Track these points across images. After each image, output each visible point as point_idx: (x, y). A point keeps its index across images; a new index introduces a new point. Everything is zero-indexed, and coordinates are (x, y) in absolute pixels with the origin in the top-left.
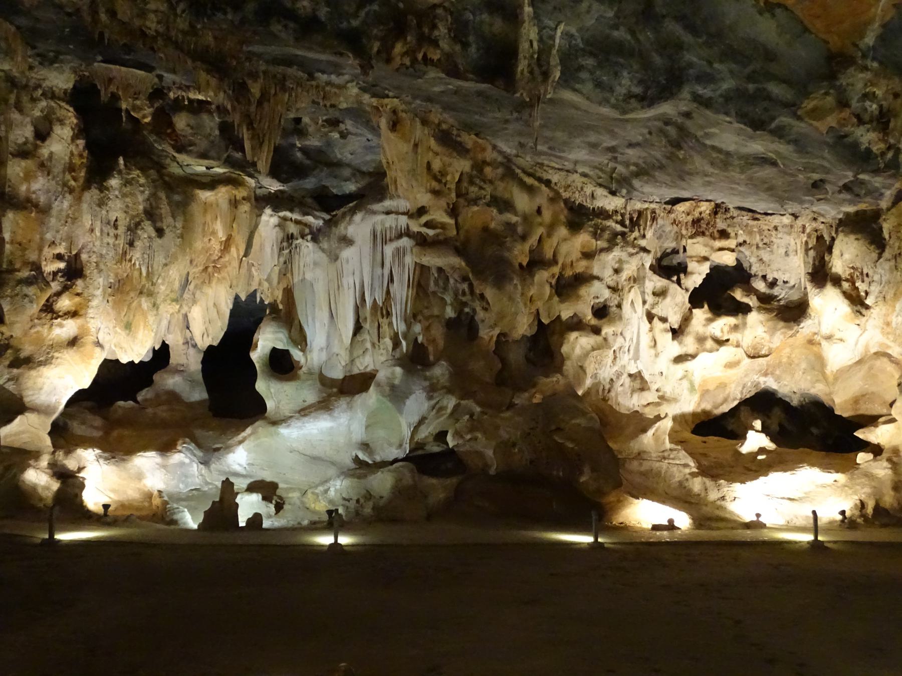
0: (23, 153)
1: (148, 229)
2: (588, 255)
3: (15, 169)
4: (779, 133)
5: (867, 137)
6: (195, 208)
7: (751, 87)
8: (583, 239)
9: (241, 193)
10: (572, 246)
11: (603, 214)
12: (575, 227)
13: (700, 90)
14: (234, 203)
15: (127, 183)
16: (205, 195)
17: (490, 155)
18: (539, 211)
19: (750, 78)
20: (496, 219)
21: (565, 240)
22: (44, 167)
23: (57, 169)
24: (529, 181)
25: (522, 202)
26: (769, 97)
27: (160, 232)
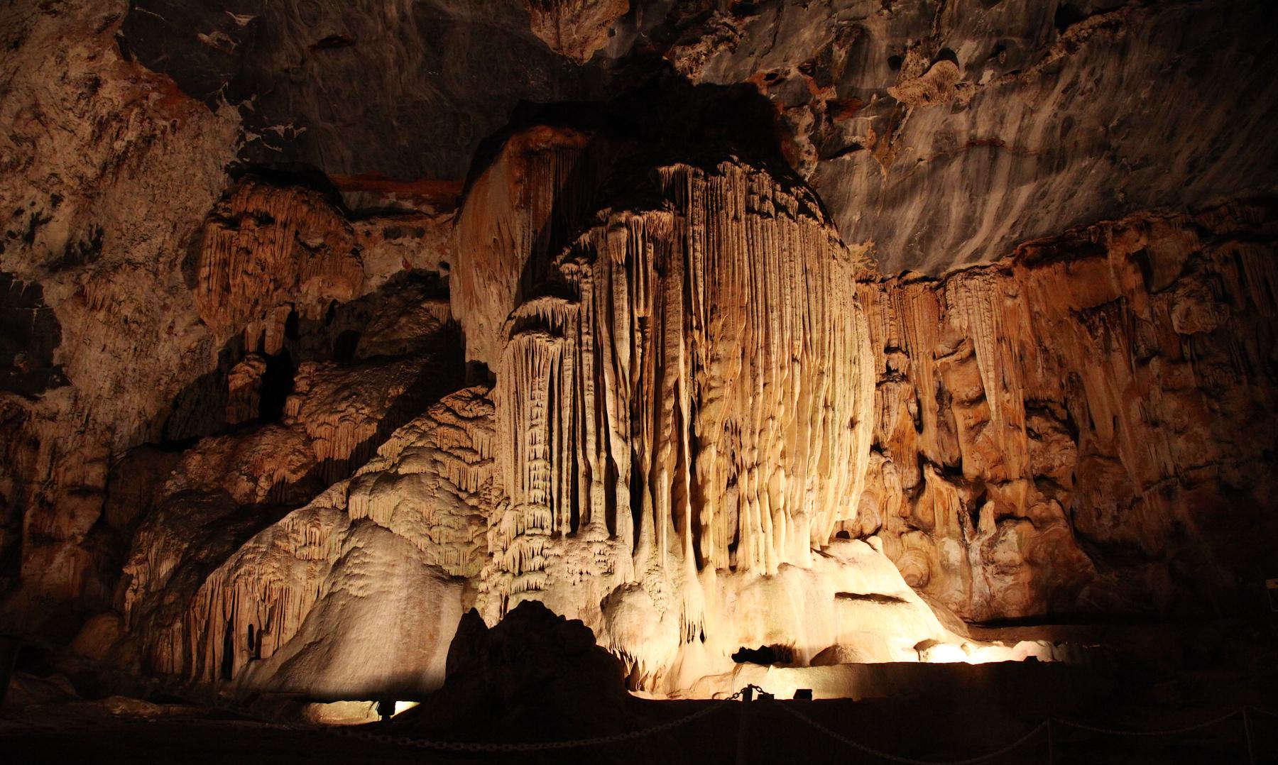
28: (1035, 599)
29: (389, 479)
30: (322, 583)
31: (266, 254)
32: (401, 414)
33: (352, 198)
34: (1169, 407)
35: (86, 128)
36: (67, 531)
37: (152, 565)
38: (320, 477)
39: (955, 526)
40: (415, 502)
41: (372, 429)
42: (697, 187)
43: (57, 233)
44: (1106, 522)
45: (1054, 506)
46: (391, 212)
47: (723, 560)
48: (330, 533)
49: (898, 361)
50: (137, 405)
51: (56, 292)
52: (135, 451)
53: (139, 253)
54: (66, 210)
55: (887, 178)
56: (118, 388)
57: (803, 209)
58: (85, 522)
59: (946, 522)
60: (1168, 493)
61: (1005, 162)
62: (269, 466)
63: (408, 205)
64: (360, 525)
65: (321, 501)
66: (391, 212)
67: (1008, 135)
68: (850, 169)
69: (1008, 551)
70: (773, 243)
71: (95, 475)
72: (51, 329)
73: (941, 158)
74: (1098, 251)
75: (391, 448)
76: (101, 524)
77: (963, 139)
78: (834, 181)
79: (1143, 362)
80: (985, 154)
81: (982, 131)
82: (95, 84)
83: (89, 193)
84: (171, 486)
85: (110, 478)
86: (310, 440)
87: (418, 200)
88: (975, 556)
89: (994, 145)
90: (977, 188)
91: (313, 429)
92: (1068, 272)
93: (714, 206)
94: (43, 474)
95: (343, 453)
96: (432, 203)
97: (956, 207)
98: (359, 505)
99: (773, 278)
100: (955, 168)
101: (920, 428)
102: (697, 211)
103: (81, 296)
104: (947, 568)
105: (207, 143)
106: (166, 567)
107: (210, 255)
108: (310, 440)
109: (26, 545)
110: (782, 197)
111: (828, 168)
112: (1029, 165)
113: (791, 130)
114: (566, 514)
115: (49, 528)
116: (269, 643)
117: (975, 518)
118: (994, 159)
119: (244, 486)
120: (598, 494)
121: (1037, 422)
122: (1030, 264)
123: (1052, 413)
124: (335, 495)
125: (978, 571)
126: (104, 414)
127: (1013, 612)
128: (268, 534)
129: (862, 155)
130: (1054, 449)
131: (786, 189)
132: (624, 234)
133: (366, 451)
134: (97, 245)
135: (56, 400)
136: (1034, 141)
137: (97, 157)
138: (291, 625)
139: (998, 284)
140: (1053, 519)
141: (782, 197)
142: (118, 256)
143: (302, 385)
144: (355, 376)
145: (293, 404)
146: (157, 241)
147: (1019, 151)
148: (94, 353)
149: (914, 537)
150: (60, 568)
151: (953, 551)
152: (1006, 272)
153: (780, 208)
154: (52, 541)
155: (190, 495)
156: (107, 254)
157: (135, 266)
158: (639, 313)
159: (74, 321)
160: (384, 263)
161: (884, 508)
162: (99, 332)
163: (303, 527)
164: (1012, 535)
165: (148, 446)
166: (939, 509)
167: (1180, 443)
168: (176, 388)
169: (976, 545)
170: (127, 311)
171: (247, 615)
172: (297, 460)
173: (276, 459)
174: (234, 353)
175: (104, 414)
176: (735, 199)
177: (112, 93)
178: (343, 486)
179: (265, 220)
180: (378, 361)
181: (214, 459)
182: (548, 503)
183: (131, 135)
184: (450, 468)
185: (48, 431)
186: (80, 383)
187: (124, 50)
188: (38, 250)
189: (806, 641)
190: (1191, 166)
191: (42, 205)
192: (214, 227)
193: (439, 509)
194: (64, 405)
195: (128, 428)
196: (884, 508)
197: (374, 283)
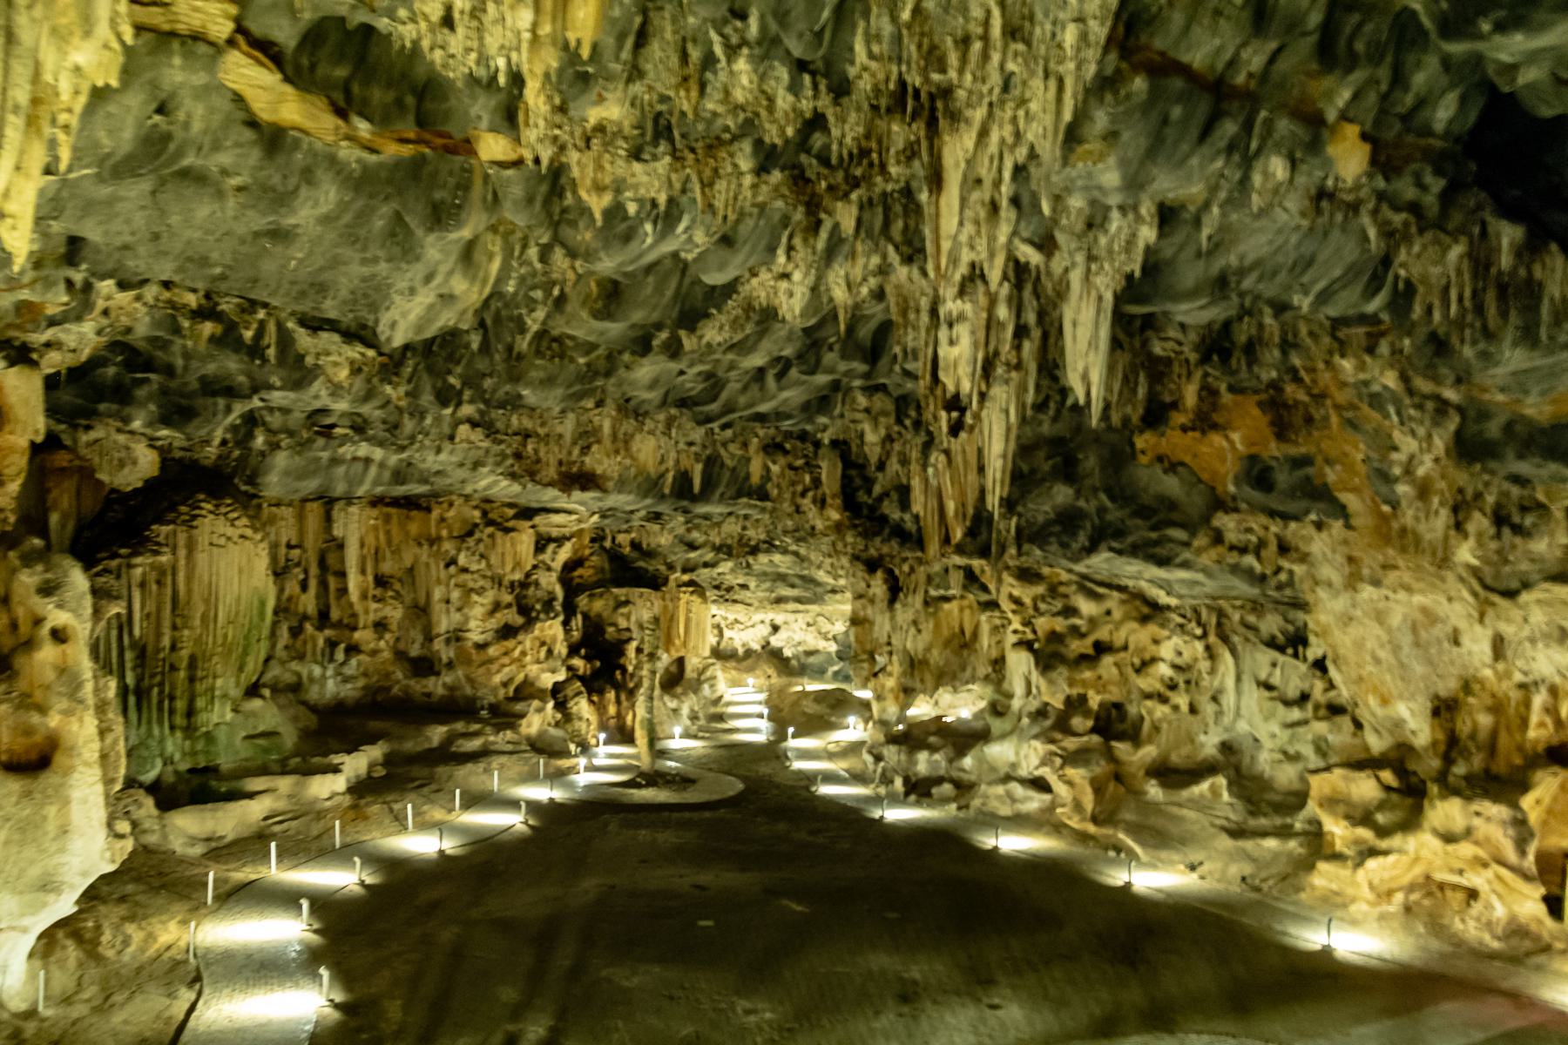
1: (913, 630)
2: (1156, 642)
4: (1185, 565)
5: (1249, 560)
6: (941, 614)
7: (1154, 535)
8: (1153, 629)
9: (966, 603)
10: (1138, 636)
11: (1168, 608)
12: (1144, 620)
13: (1115, 545)
14: (961, 610)
15: (904, 605)
16: (946, 606)
17: (1065, 576)
18: (1108, 613)
19: (1154, 528)
20: (1060, 624)
21: (1134, 631)
22: (872, 601)
23: (877, 600)
24: (1101, 590)
25: (1087, 607)
26: (1171, 540)
27: (919, 631)
39: (319, 658)
42: (182, 538)
59: (314, 653)
88: (329, 673)
93: (191, 547)
102: (182, 553)
104: (311, 680)
112: (387, 475)
117: (332, 654)
118: (366, 469)
166: (309, 647)
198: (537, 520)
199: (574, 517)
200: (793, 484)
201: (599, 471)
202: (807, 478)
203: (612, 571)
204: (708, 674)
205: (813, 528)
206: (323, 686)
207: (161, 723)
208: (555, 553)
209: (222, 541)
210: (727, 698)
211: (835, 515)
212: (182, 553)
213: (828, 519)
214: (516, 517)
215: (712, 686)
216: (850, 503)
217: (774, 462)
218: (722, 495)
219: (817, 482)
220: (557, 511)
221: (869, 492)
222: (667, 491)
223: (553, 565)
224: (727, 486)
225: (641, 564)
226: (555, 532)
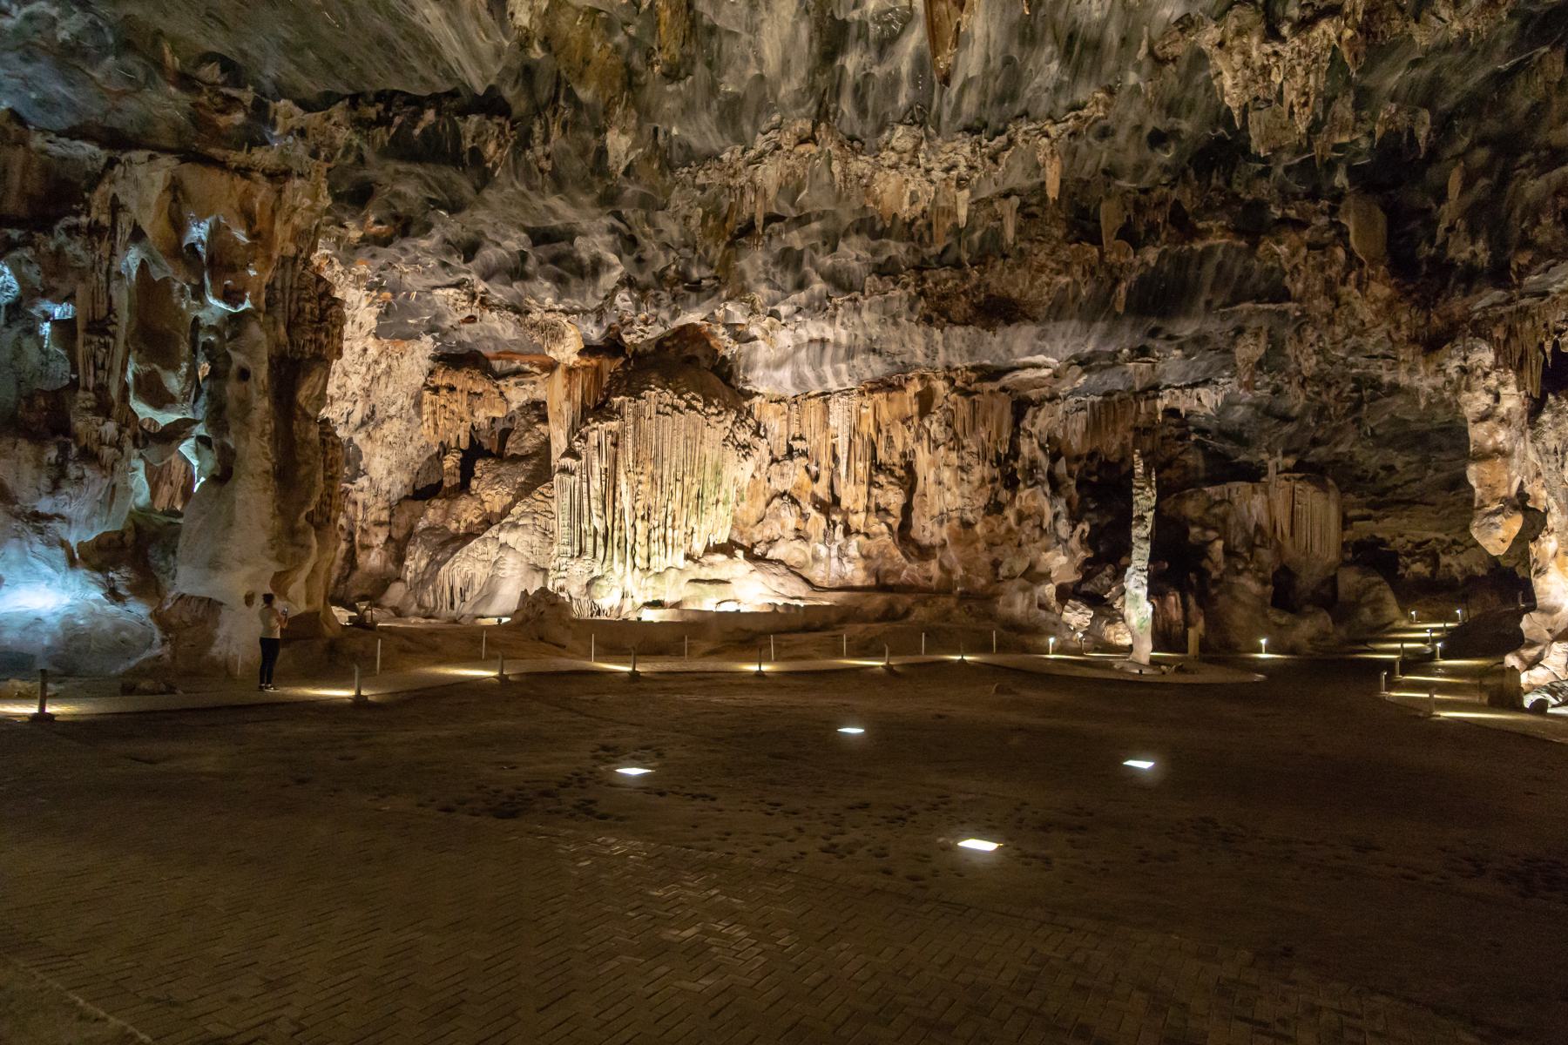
0: (1484, 417)
3: (1477, 433)
23: (1515, 418)
28: (869, 576)
29: (515, 526)
30: (489, 570)
31: (454, 407)
32: (525, 491)
33: (497, 365)
34: (947, 475)
35: (364, 369)
36: (375, 542)
37: (416, 561)
38: (488, 521)
40: (527, 538)
41: (510, 499)
42: (629, 408)
43: (357, 417)
44: (927, 534)
45: (884, 527)
46: (518, 372)
47: (645, 565)
48: (492, 548)
49: (797, 445)
50: (397, 484)
51: (358, 438)
52: (399, 502)
53: (392, 411)
54: (359, 405)
55: (774, 355)
56: (390, 473)
57: (690, 407)
58: (382, 538)
60: (941, 523)
61: (829, 350)
62: (465, 516)
63: (527, 367)
64: (504, 546)
65: (487, 534)
66: (518, 372)
67: (829, 334)
68: (756, 349)
69: (853, 551)
70: (668, 427)
71: (384, 516)
72: (358, 452)
73: (797, 348)
74: (901, 388)
75: (516, 510)
76: (390, 538)
77: (806, 339)
78: (748, 355)
79: (937, 447)
80: (817, 347)
81: (815, 335)
82: (365, 350)
83: (367, 393)
84: (422, 524)
85: (391, 516)
86: (483, 502)
87: (532, 364)
88: (834, 553)
89: (823, 341)
90: (816, 364)
91: (484, 497)
92: (888, 399)
93: (638, 415)
94: (360, 516)
95: (498, 510)
96: (540, 366)
97: (808, 373)
98: (503, 537)
99: (667, 446)
100: (803, 354)
101: (816, 479)
102: (629, 419)
103: (369, 436)
105: (418, 354)
106: (423, 563)
107: (427, 408)
108: (483, 502)
109: (358, 551)
110: (677, 401)
111: (745, 347)
112: (842, 352)
113: (714, 335)
114: (577, 548)
115: (366, 541)
116: (468, 596)
118: (823, 349)
119: (454, 525)
120: (590, 541)
121: (882, 479)
122: (871, 391)
123: (892, 473)
124: (494, 530)
125: (835, 562)
126: (385, 486)
127: (858, 583)
128: (465, 549)
129: (760, 342)
130: (890, 494)
131: (680, 397)
132: (595, 433)
133: (506, 512)
134: (373, 412)
135: (362, 482)
136: (844, 340)
137: (369, 378)
138: (477, 588)
139: (856, 401)
140: (882, 534)
141: (677, 401)
142: (383, 415)
143: (478, 474)
144: (502, 470)
145: (474, 483)
146: (399, 403)
147: (837, 345)
148: (378, 459)
149: (797, 543)
150: (374, 560)
151: (823, 551)
152: (862, 393)
153: (675, 408)
154: (369, 547)
155: (430, 529)
156: (378, 416)
157: (391, 418)
158: (604, 465)
159: (366, 448)
160: (518, 396)
161: (783, 527)
162: (378, 450)
163: (480, 546)
164: (854, 540)
165: (406, 497)
167: (948, 496)
168: (417, 467)
169: (834, 547)
170: (390, 439)
171: (458, 585)
172: (478, 512)
173: (467, 512)
174: (445, 449)
175: (385, 486)
176: (650, 410)
177: (373, 351)
178: (497, 527)
179: (452, 389)
180: (515, 459)
181: (440, 512)
182: (571, 544)
183: (383, 366)
184: (541, 521)
185: (360, 497)
186: (373, 474)
187: (377, 336)
188: (351, 426)
189: (669, 598)
190: (927, 356)
191: (349, 406)
192: (427, 393)
193: (536, 539)
194: (366, 484)
195: (398, 491)
196: (783, 527)
197: (514, 406)
198: (1007, 380)
199: (1045, 372)
200: (1322, 268)
201: (1015, 294)
202: (1340, 253)
203: (1207, 470)
204: (1372, 596)
205: (1363, 323)
206: (828, 565)
207: (624, 561)
208: (1035, 417)
209: (668, 409)
210: (1397, 624)
211: (1381, 290)
212: (629, 419)
213: (1376, 300)
214: (980, 379)
215: (1375, 611)
216: (1401, 264)
217: (1279, 243)
218: (1208, 303)
219: (1350, 254)
220: (1024, 367)
221: (1431, 241)
222: (1120, 309)
223: (1034, 430)
224: (1213, 288)
225: (1243, 457)
226: (1033, 394)
